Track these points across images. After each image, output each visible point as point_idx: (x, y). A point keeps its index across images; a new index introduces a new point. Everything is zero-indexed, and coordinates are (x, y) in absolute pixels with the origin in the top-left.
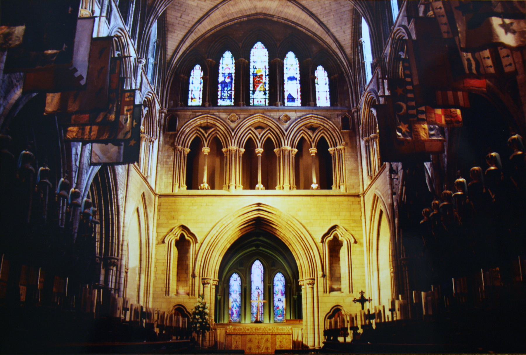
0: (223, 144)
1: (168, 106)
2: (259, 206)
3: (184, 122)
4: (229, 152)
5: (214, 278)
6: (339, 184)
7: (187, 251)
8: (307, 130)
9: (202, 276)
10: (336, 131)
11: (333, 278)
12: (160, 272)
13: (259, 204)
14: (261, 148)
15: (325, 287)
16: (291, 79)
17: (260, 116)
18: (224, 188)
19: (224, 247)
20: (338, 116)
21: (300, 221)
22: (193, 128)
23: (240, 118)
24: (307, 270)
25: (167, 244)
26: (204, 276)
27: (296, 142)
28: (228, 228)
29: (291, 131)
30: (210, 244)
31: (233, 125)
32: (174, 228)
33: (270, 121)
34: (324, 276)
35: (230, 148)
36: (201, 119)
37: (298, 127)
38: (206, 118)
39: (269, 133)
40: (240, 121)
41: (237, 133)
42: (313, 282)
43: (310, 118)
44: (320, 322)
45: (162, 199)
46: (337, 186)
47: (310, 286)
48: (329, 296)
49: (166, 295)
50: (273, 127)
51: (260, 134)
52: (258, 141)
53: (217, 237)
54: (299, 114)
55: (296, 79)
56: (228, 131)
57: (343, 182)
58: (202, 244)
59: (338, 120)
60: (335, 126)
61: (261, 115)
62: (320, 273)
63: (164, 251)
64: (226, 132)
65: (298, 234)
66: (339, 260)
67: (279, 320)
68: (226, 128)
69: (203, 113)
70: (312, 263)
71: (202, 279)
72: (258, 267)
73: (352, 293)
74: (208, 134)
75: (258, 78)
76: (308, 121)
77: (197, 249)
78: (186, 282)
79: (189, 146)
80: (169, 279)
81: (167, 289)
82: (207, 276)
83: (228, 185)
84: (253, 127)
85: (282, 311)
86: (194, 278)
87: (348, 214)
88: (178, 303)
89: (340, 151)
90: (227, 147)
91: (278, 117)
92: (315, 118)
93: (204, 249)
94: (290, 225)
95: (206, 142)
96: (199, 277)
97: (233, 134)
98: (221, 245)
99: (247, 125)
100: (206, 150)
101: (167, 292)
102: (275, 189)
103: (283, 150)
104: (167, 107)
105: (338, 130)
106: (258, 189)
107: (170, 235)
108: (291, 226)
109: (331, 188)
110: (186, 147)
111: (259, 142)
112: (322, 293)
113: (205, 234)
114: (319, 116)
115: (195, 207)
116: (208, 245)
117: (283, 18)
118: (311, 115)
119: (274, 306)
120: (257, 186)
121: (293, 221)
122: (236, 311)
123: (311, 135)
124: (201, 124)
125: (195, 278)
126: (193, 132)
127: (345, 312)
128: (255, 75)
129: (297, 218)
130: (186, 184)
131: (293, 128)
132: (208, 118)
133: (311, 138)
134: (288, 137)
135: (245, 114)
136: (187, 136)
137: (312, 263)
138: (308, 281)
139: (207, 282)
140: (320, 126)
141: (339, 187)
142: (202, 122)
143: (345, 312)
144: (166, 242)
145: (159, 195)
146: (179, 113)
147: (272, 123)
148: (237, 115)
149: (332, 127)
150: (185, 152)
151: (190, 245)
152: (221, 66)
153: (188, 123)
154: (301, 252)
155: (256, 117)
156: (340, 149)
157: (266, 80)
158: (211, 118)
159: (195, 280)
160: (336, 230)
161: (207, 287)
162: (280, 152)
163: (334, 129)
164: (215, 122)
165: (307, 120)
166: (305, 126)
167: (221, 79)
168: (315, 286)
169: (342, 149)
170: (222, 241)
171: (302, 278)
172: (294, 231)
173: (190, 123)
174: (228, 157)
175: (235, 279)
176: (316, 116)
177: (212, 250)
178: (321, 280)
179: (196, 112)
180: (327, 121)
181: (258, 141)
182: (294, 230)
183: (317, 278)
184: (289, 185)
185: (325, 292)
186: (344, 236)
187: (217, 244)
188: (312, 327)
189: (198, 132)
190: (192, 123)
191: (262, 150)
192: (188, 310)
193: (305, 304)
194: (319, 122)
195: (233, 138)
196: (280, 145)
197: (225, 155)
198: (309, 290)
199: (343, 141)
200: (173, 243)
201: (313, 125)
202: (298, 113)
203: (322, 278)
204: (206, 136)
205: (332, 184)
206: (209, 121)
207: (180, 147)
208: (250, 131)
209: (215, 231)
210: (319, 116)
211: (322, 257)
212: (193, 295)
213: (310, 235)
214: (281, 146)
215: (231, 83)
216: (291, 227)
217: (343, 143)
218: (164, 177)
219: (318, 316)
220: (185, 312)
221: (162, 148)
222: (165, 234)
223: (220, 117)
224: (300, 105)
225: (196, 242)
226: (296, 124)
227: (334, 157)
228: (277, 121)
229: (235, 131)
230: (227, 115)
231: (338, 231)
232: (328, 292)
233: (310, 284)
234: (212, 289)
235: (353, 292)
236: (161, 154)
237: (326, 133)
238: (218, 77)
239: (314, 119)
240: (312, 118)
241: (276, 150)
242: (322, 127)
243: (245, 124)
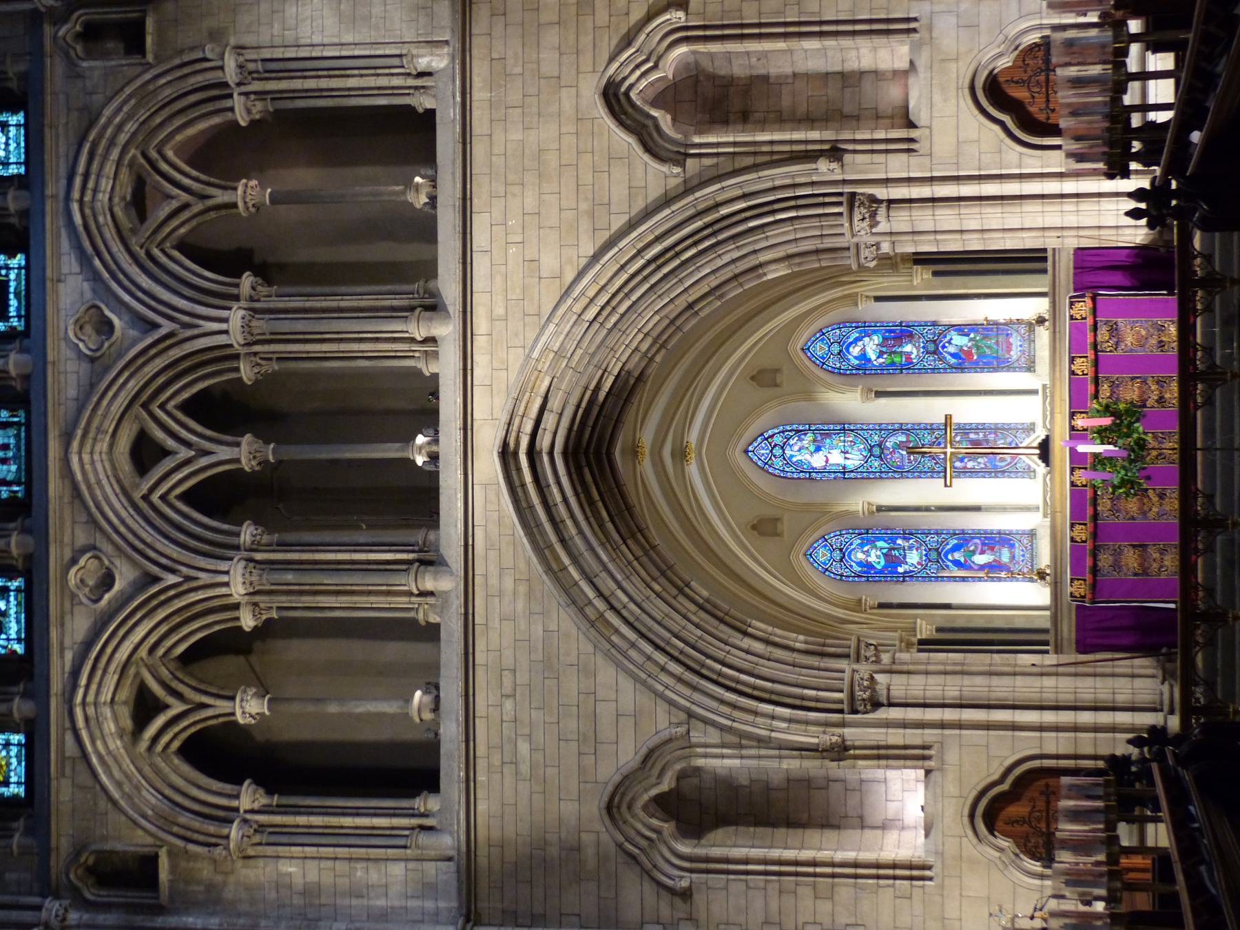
0: (217, 628)
1: (31, 894)
2: (516, 453)
3: (113, 816)
4: (257, 598)
5: (847, 656)
6: (409, 74)
7: (727, 786)
8: (151, 224)
9: (841, 711)
10: (151, 87)
11: (848, 109)
12: (825, 907)
13: (507, 455)
14: (238, 445)
15: (888, 147)
17: (80, 453)
18: (434, 618)
19: (703, 614)
20: (74, 74)
21: (583, 262)
22: (140, 771)
23: (94, 548)
24: (810, 229)
25: (694, 876)
26: (841, 702)
27: (208, 278)
28: (619, 593)
29: (153, 303)
30: (695, 679)
31: (124, 577)
32: (620, 846)
33: (105, 402)
34: (835, 152)
35: (238, 590)
36: (97, 733)
37: (134, 271)
38: (91, 711)
39: (162, 407)
40: (108, 548)
41: (163, 561)
42: (862, 203)
43: (88, 211)
44: (1046, 170)
45: (483, 905)
46: (416, 88)
47: (882, 211)
48: (930, 128)
49: (930, 879)
50: (133, 386)
51: (166, 453)
52: (204, 461)
53: (657, 647)
56: (155, 602)
57: (400, 56)
58: (691, 715)
59: (96, 73)
60: (128, 91)
61: (75, 445)
62: (825, 169)
63: (726, 888)
64: (161, 614)
65: (645, 273)
66: (765, 79)
67: (1023, 352)
68: (138, 615)
69: (68, 724)
70: (776, 206)
71: (855, 712)
72: (778, 451)
73: (915, 19)
74: (170, 700)
76: (101, 219)
77: (714, 736)
78: (864, 787)
79: (228, 788)
80: (856, 865)
81: (899, 872)
82: (842, 691)
83: (414, 599)
84: (137, 486)
85: (985, 337)
86: (846, 749)
87: (551, 37)
88: (966, 820)
89: (251, 66)
90: (236, 607)
91: (85, 366)
92: (91, 185)
93: (714, 704)
94: (603, 308)
95: (204, 706)
96: (843, 724)
97: (172, 579)
98: (697, 626)
99: (124, 514)
101: (915, 873)
102: (435, 377)
103: (250, 338)
104: (36, 900)
105: (148, 76)
106: (434, 458)
107: (655, 866)
108: (608, 302)
109: (431, 113)
110: (235, 803)
111: (208, 453)
112: (914, 160)
113: (646, 700)
114: (81, 168)
115: (524, 748)
116: (695, 688)
118: (75, 207)
120: (420, 460)
121: (583, 293)
122: (982, 552)
123: (175, 204)
124: (121, 733)
125: (848, 743)
126: (158, 771)
127: (1001, 55)
129: (569, 276)
130: (413, 795)
131: (140, 294)
132: (90, 698)
133: (186, 206)
134: (186, 319)
135: (74, 522)
136: (179, 798)
137: (776, 206)
138: (861, 226)
139: (868, 687)
140: (126, 162)
141: (421, 75)
142: (110, 727)
143: (1001, 55)
144: (684, 884)
145: (468, 920)
147: (115, 395)
148: (74, 561)
149: (133, 102)
150: (256, 806)
151: (698, 770)
153: (116, 795)
154: (727, 258)
155: (88, 467)
156: (241, 67)
158: (94, 687)
159: (857, 743)
160: (627, 94)
161: (889, 690)
162: (255, 354)
163: (143, 95)
164: (112, 668)
165: (98, 228)
166: (126, 233)
168: (881, 193)
169: (241, 59)
170: (677, 623)
171: (846, 254)
172: (632, 290)
173: (119, 785)
174: (284, 601)
175: (837, 555)
176: (78, 181)
177: (718, 667)
178: (860, 166)
179: (62, 759)
180: (105, 127)
181: (204, 461)
182: (626, 290)
183: (844, 182)
184: (419, 310)
185: (908, 147)
186: (654, 59)
187: (694, 648)
188: (1069, 206)
189: (159, 748)
190: (117, 774)
191: (248, 437)
192: (996, 777)
193: (966, 236)
194: (110, 168)
195: (188, 579)
196: (226, 356)
197: (274, 615)
198: (901, 220)
199: (200, 55)
200: (684, 848)
201: (123, 198)
202: (65, 270)
203: (848, 158)
204: (177, 708)
205: (410, 109)
206: (106, 695)
207: (235, 832)
208: (155, 498)
209: (633, 653)
210: (81, 168)
211: (749, 161)
212: (926, 752)
213: (647, 214)
214: (228, 351)
216: (614, 303)
217: (209, 55)
218: (381, 902)
219: (1021, 177)
220: (1005, 787)
221: (239, 915)
222: (649, 888)
223: (88, 645)
224: (19, 260)
226: (121, 276)
227: (277, 96)
228: (107, 369)
229: (155, 570)
230: (77, 609)
231: (631, 86)
232: (913, 134)
233: (873, 215)
234: (895, 667)
235: (912, 15)
236: (266, 917)
237: (162, 135)
239: (95, 191)
240: (87, 198)
241: (246, 372)
242: (133, 151)
243: (123, 522)
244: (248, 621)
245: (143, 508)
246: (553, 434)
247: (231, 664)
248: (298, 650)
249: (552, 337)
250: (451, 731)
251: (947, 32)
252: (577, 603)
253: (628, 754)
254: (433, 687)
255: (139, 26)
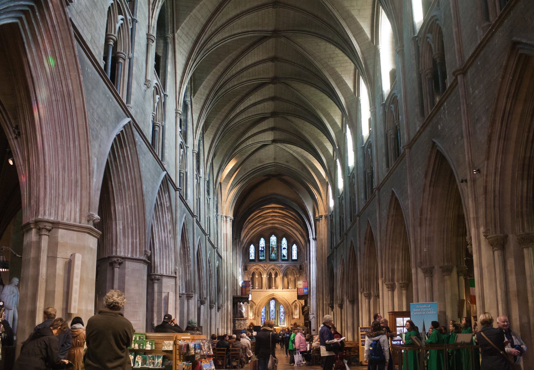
13: (273, 294)
16: (284, 248)
27: (285, 274)
31: (265, 268)
54: (286, 265)
55: (286, 249)
75: (273, 248)
100: (257, 276)
117: (281, 228)
119: (280, 318)
128: (272, 247)
146: (248, 264)
152: (260, 244)
157: (275, 249)
167: (260, 249)
215: (264, 250)
225: (256, 305)
238: (259, 248)
241: (279, 276)
244: (262, 276)
245: (270, 269)
246: (274, 297)
247: (259, 274)
248: (260, 278)
249: (281, 297)
250: (256, 290)
251: (299, 321)
252: (264, 298)
253: (254, 302)
254: (258, 289)
255: (301, 269)
